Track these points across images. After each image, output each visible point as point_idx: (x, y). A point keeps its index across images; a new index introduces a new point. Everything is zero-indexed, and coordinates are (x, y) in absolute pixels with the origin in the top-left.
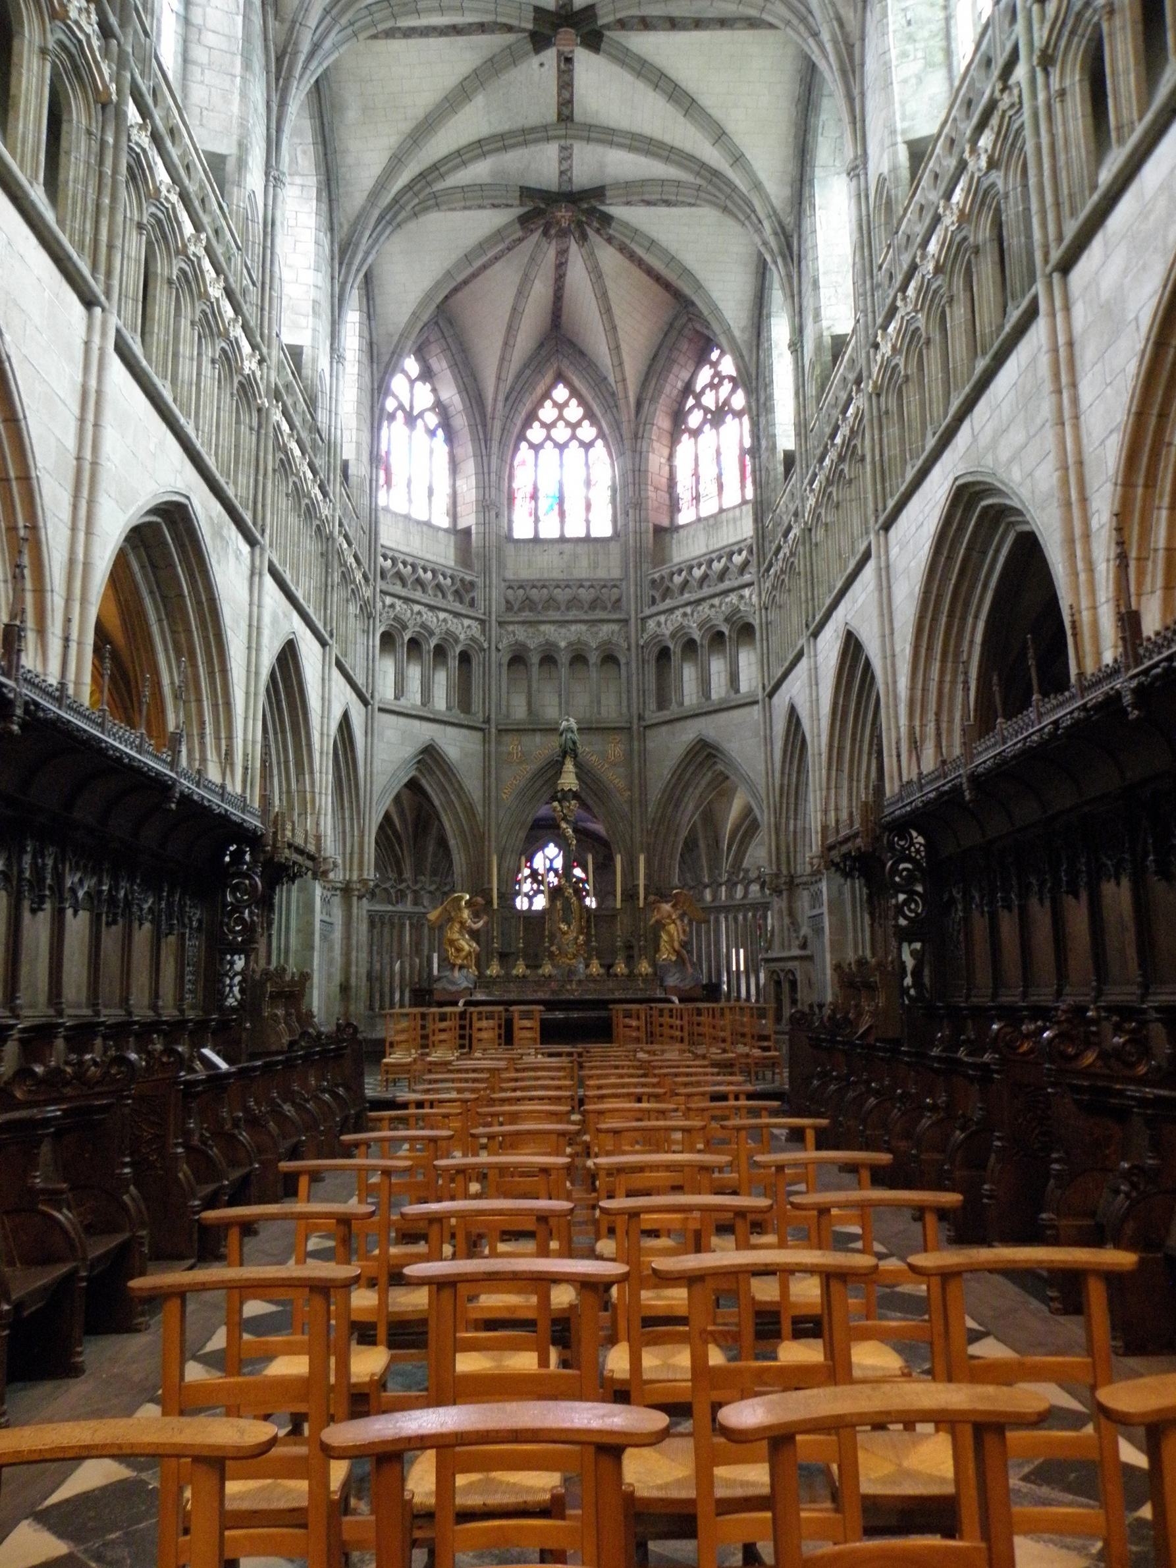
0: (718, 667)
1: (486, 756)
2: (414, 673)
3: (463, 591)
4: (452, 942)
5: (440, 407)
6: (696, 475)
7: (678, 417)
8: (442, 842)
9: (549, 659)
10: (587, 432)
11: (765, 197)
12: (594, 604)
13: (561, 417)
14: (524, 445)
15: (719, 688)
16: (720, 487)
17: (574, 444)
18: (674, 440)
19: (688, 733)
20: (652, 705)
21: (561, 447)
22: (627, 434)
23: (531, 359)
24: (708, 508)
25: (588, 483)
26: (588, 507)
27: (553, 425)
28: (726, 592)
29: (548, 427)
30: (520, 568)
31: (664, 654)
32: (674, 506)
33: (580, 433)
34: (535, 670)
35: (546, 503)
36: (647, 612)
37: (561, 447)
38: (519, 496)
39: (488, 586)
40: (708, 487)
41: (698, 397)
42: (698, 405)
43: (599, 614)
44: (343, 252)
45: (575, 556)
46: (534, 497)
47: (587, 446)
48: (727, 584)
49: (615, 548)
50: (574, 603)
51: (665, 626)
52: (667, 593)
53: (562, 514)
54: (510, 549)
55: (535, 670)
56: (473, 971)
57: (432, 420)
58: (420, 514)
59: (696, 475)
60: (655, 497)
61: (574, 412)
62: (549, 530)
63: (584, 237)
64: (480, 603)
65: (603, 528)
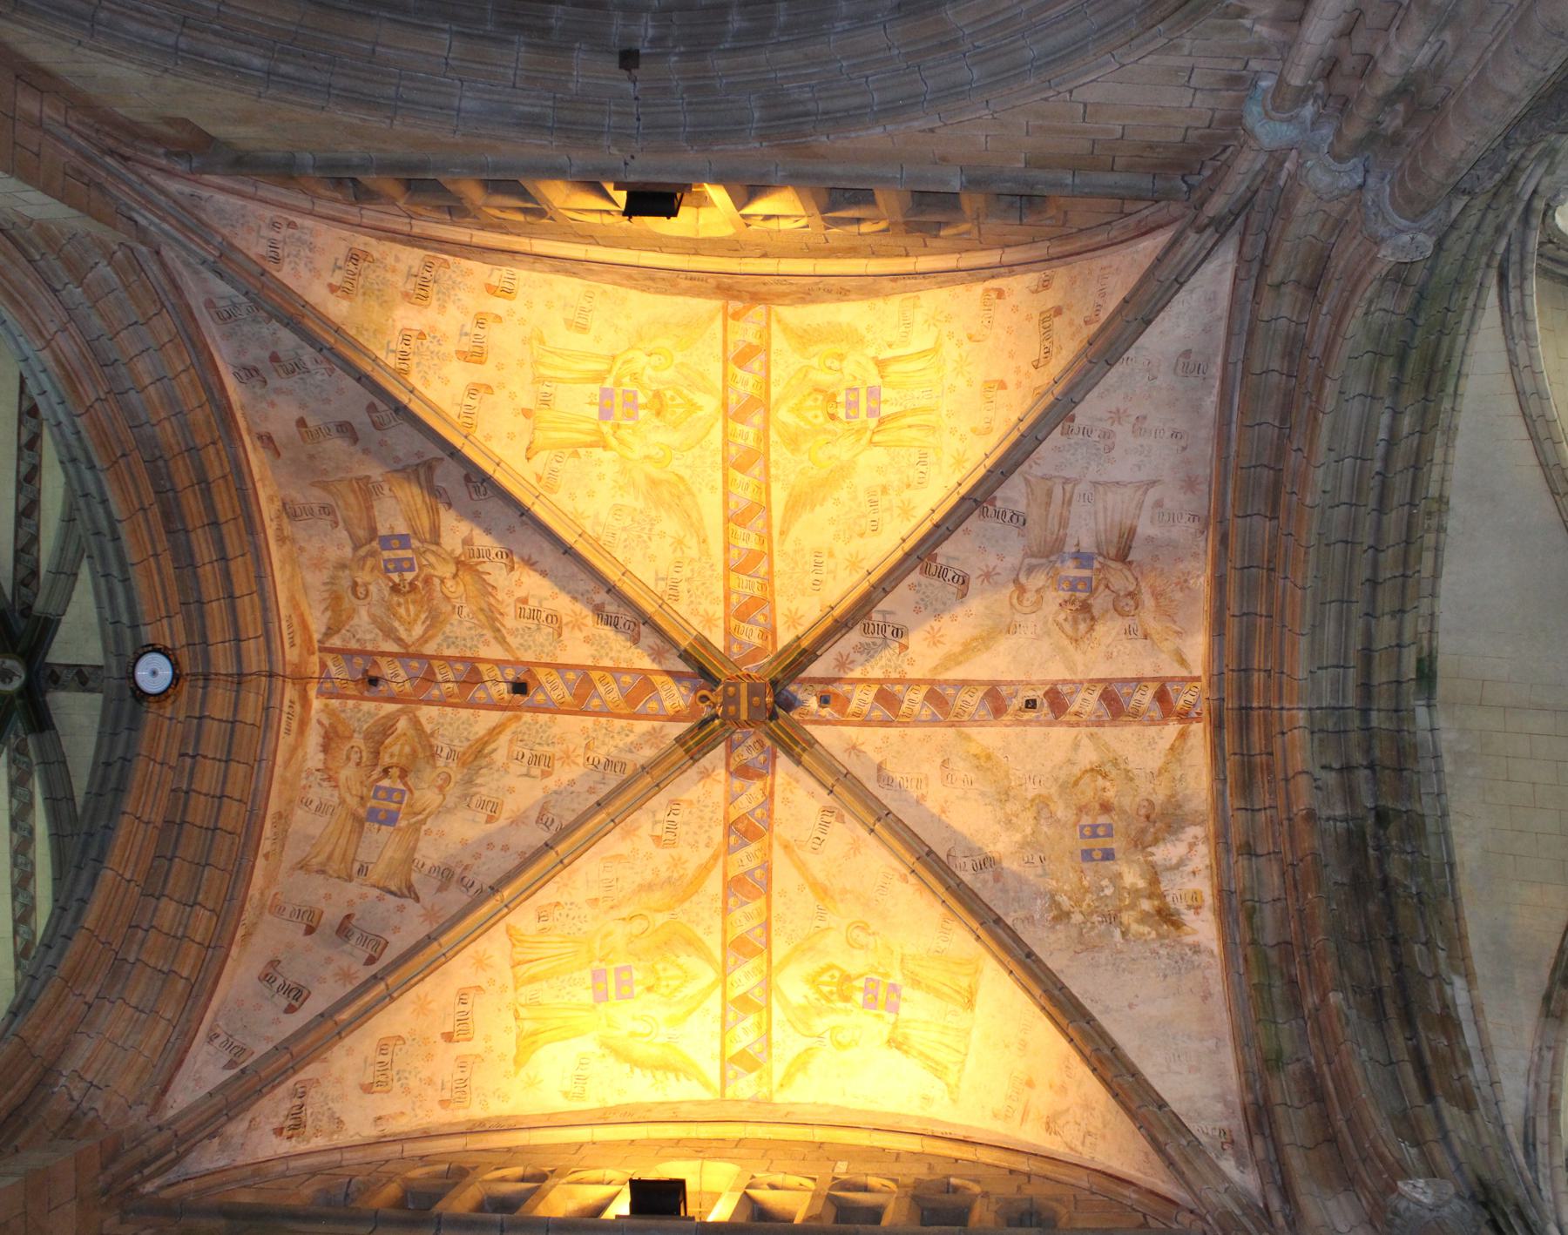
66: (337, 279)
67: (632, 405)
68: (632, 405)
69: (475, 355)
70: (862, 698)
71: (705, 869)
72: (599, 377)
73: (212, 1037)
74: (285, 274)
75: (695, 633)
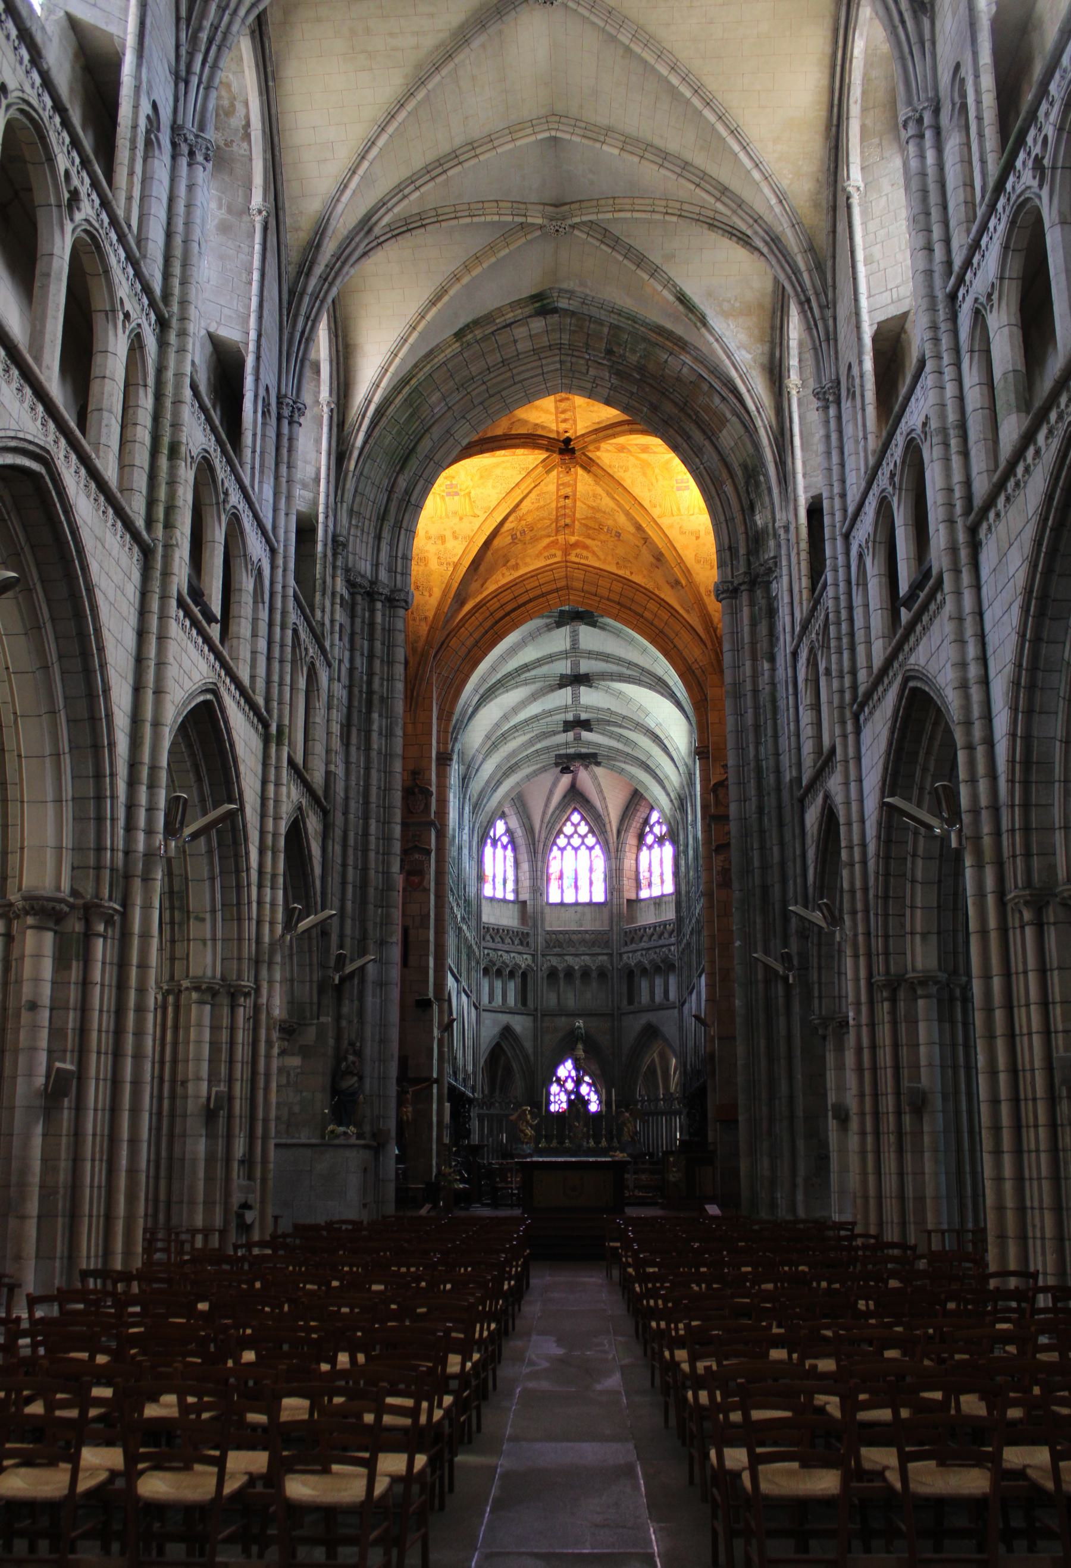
0: (659, 981)
1: (535, 1028)
2: (498, 984)
3: (522, 938)
4: (522, 1131)
5: (509, 831)
6: (650, 871)
7: (641, 837)
8: (508, 1070)
9: (569, 973)
10: (591, 840)
11: (671, 782)
12: (593, 944)
13: (576, 832)
14: (555, 848)
15: (659, 997)
16: (662, 882)
17: (583, 847)
18: (639, 848)
19: (643, 1019)
20: (625, 1002)
21: (576, 849)
22: (612, 850)
23: (560, 804)
24: (656, 892)
25: (591, 870)
26: (591, 883)
27: (572, 836)
28: (662, 946)
29: (569, 837)
30: (553, 923)
31: (631, 974)
32: (638, 887)
33: (586, 841)
34: (562, 982)
35: (568, 881)
36: (623, 950)
37: (576, 849)
38: (553, 877)
39: (536, 935)
40: (656, 879)
41: (651, 827)
42: (651, 831)
43: (597, 950)
44: (474, 808)
45: (584, 914)
46: (561, 877)
47: (590, 849)
48: (661, 942)
49: (606, 911)
50: (583, 942)
51: (631, 960)
52: (632, 941)
53: (576, 887)
54: (547, 910)
55: (562, 982)
56: (532, 1145)
57: (505, 840)
58: (499, 895)
59: (650, 871)
60: (628, 884)
61: (583, 829)
62: (569, 898)
63: (586, 767)
64: (532, 945)
65: (599, 897)
66: (426, 594)
67: (451, 486)
68: (451, 486)
69: (443, 539)
70: (563, 426)
71: (637, 458)
72: (443, 498)
73: (688, 611)
74: (431, 614)
75: (540, 469)
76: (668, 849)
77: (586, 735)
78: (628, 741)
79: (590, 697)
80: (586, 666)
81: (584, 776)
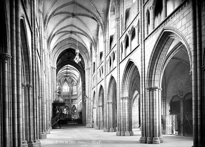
0: (75, 100)
19: (73, 105)
31: (72, 100)
51: (73, 98)
61: (67, 84)
65: (68, 91)
76: (76, 86)
77: (67, 74)
78: (72, 75)
79: (68, 71)
80: (68, 68)
81: (67, 78)
